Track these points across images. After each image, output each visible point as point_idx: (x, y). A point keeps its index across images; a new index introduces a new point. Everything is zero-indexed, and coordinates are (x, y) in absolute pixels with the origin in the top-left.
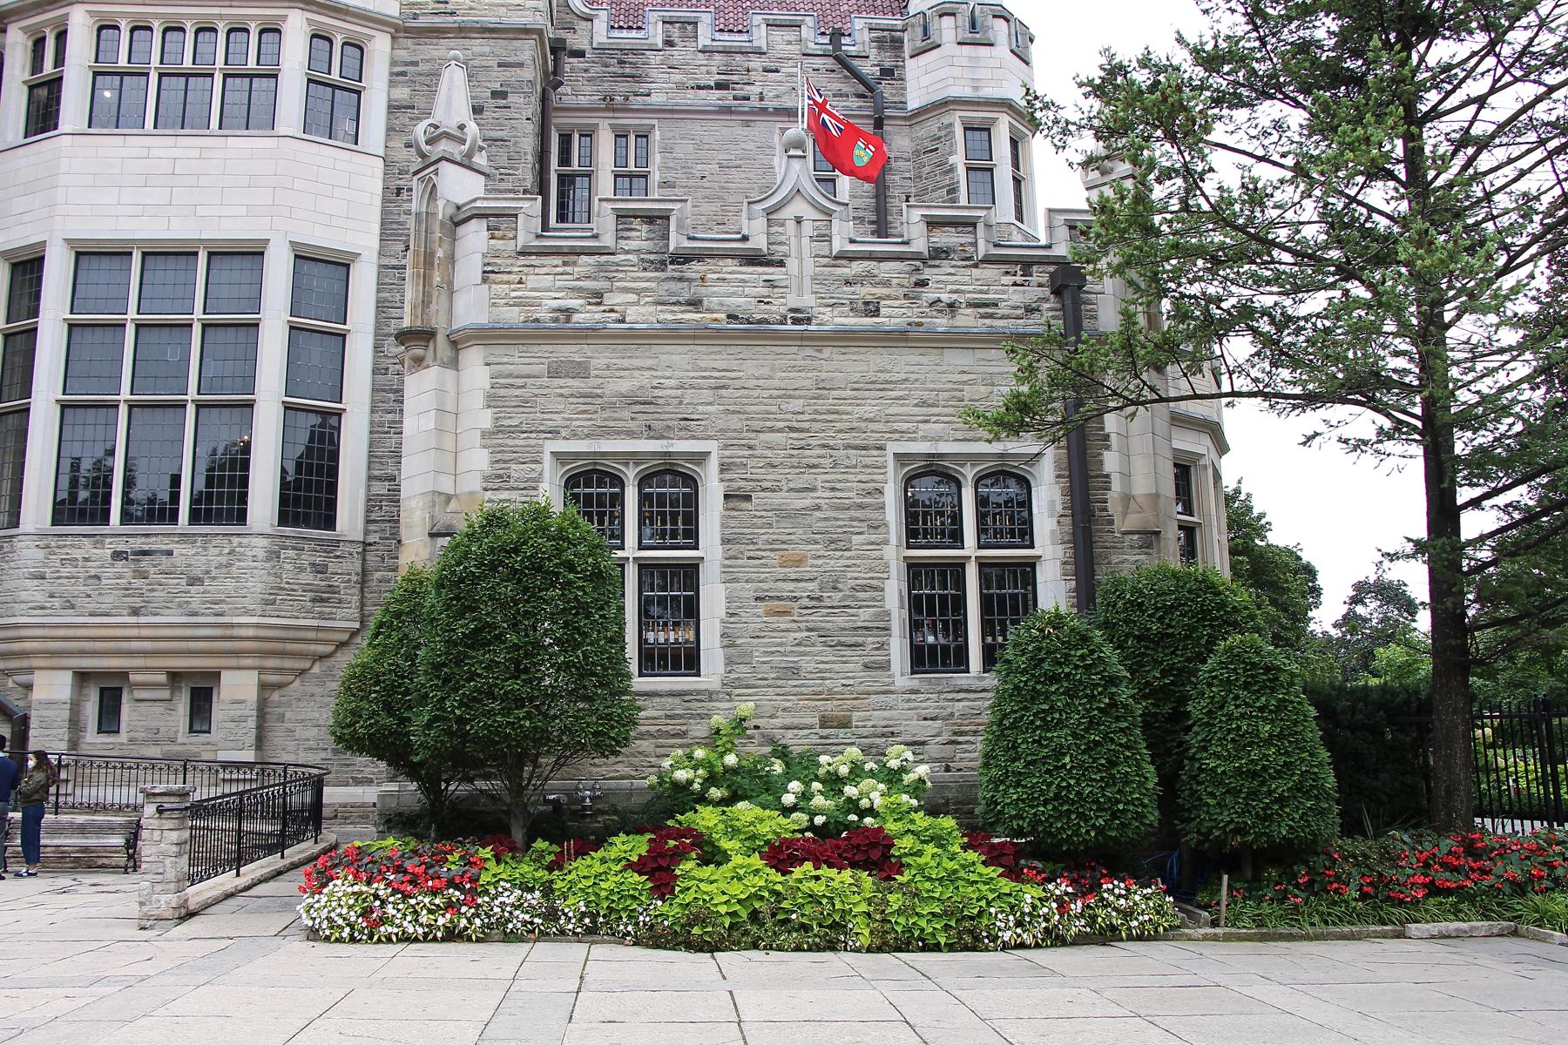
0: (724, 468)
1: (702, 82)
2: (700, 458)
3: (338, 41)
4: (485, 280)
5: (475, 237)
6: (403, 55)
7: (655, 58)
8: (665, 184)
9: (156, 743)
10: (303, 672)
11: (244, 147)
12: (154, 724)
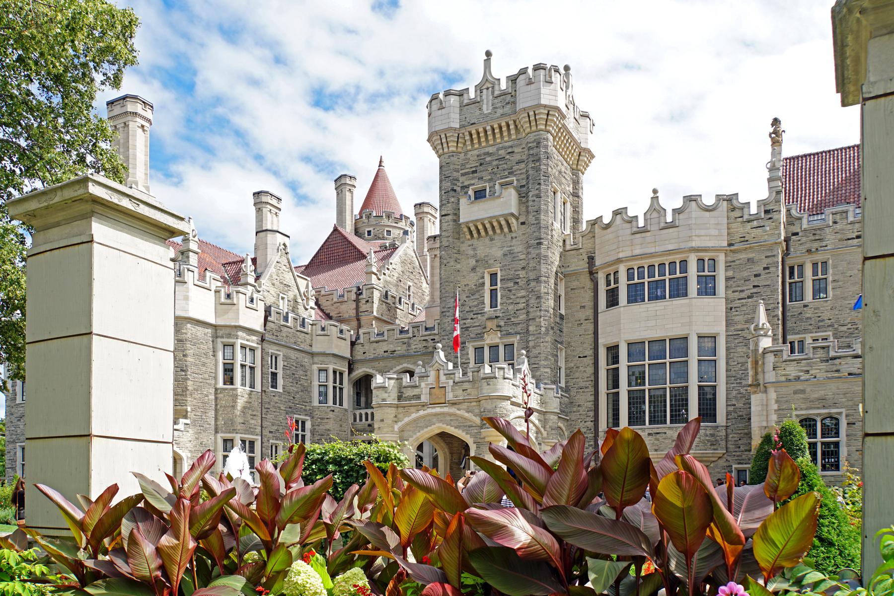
0: (847, 416)
1: (850, 237)
2: (840, 414)
7: (827, 230)
11: (679, 302)
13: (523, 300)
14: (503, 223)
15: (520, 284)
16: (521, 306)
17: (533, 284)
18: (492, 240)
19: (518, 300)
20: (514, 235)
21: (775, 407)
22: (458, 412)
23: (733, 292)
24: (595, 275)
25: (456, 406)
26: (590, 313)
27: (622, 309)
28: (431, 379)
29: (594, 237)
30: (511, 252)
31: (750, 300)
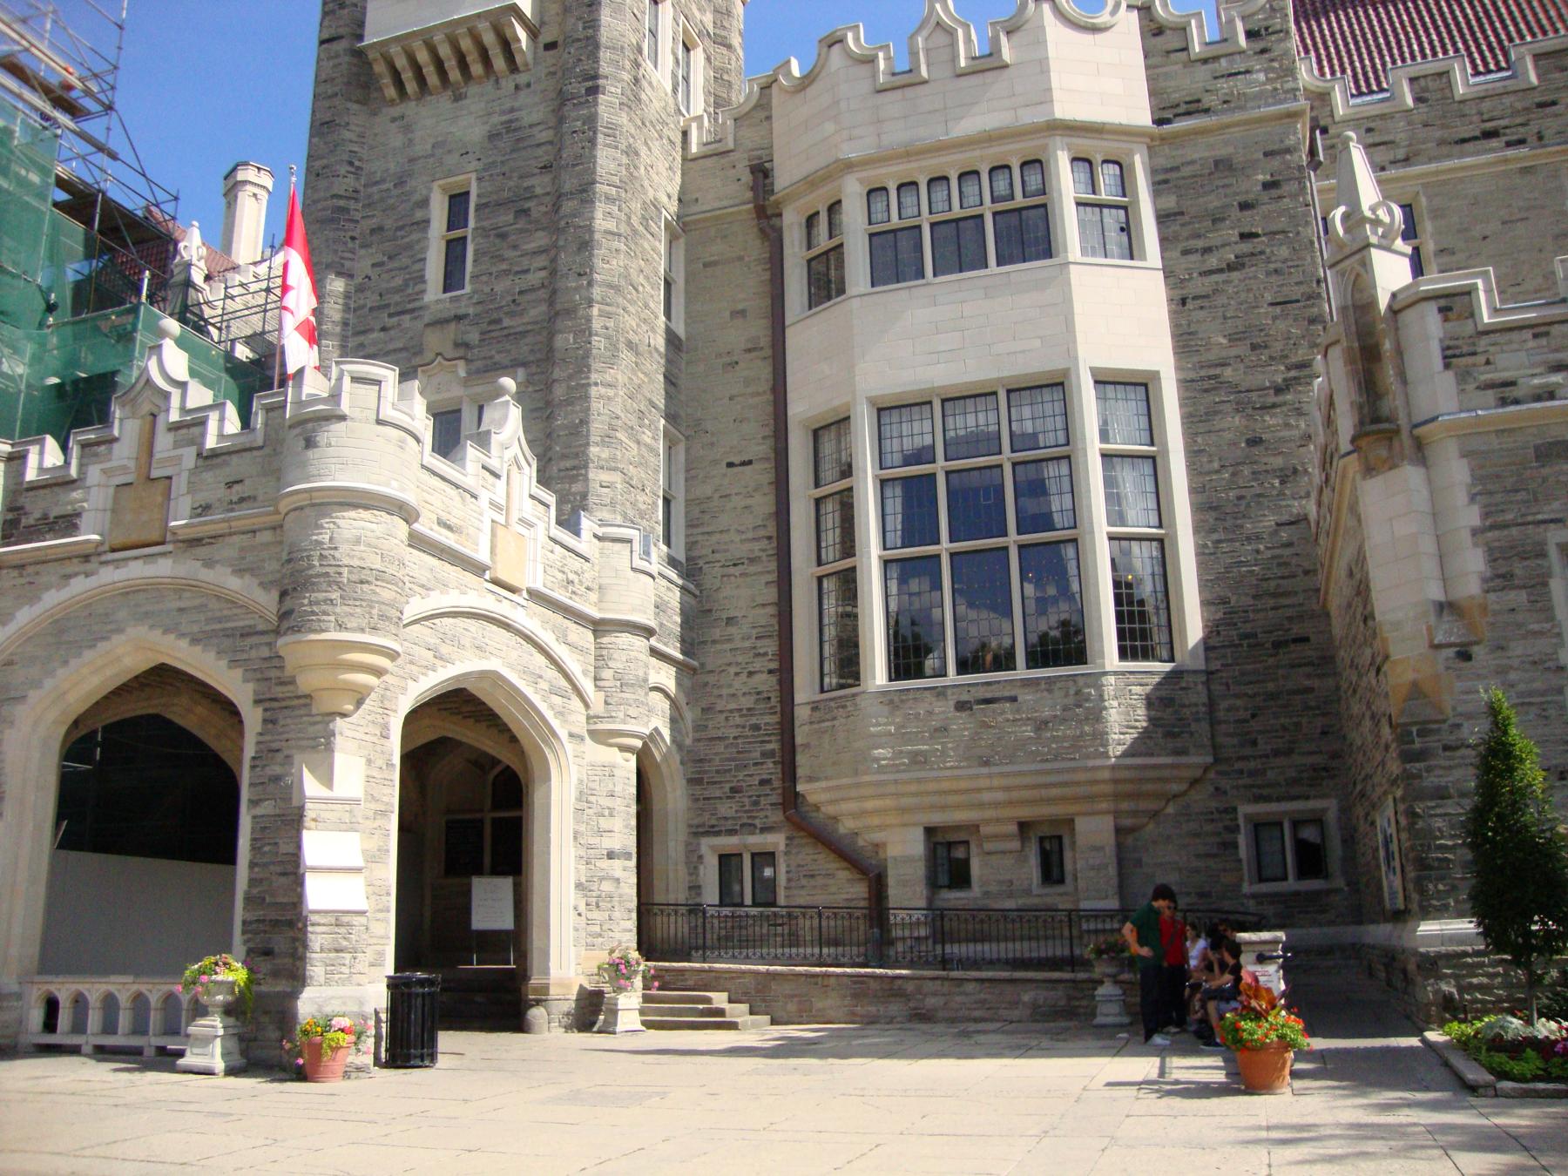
3: (1098, 159)
4: (1447, 366)
5: (1429, 328)
6: (1162, 162)
8: (1441, 251)
9: (1011, 895)
10: (1155, 815)
12: (1008, 877)
13: (541, 261)
14: (489, 39)
15: (534, 214)
16: (535, 278)
17: (568, 206)
18: (458, 98)
19: (525, 262)
20: (522, 78)
21: (1471, 516)
22: (207, 575)
23: (1185, 252)
24: (775, 221)
25: (202, 551)
26: (759, 329)
27: (855, 303)
28: (124, 452)
29: (769, 118)
30: (510, 127)
31: (1235, 275)
